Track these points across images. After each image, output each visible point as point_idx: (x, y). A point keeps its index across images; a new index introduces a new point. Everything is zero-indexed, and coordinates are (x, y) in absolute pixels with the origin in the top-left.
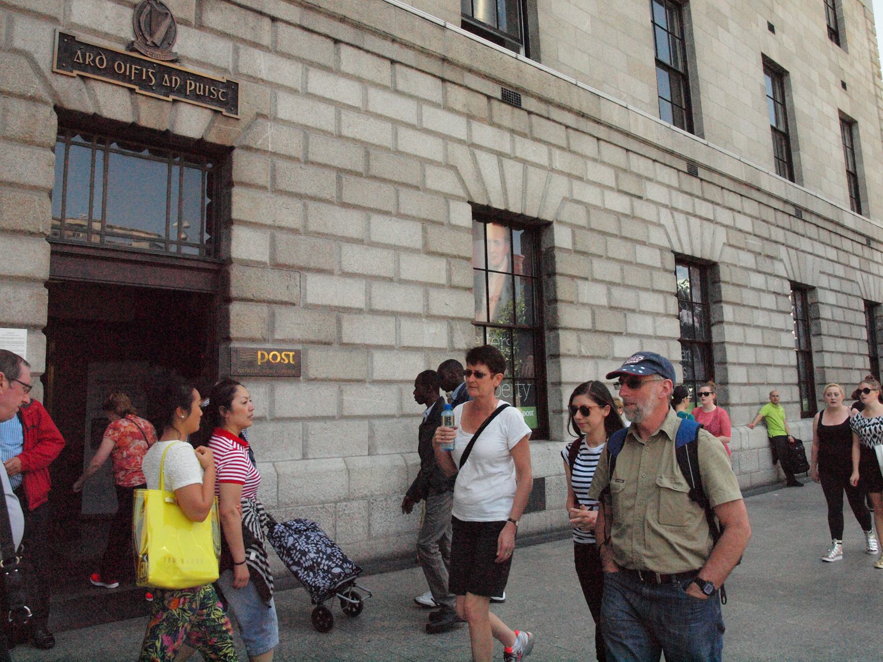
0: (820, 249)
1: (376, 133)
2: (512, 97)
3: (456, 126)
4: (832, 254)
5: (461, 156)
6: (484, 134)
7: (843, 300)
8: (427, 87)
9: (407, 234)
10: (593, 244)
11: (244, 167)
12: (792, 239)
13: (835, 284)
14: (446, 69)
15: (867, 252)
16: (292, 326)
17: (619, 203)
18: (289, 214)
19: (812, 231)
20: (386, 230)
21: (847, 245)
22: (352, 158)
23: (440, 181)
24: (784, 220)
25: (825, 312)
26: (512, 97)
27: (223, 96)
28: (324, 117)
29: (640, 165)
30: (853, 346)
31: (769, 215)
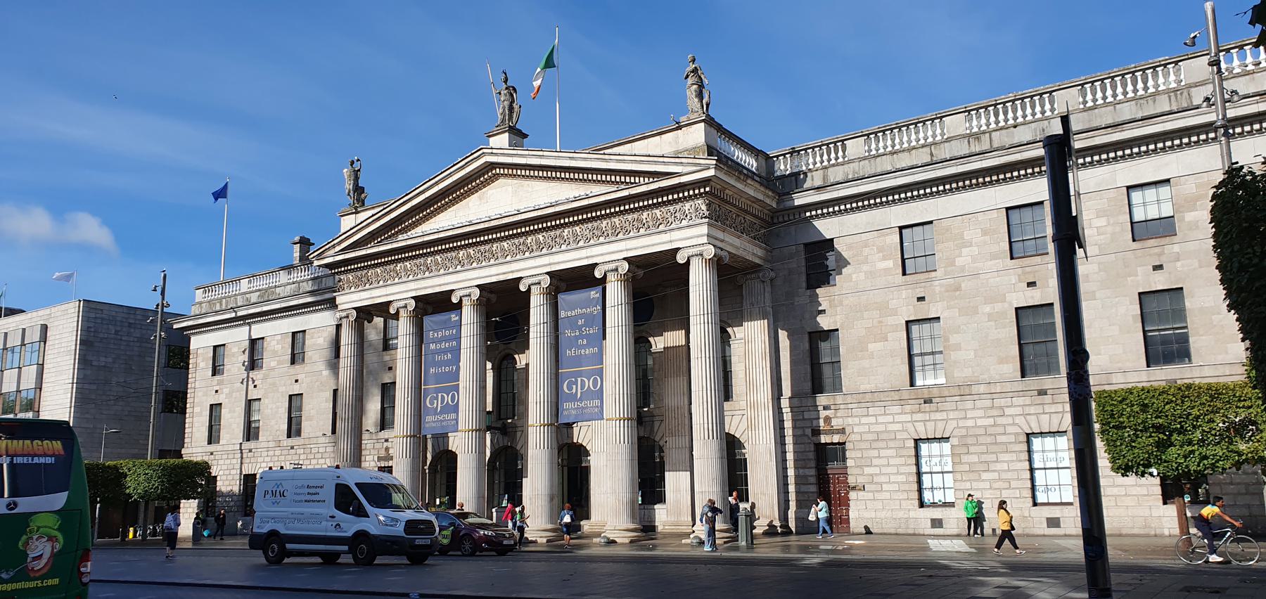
1: (881, 428)
5: (910, 427)
6: (919, 416)
8: (897, 409)
11: (848, 446)
16: (861, 480)
17: (991, 421)
23: (905, 435)
27: (842, 431)
29: (1002, 402)
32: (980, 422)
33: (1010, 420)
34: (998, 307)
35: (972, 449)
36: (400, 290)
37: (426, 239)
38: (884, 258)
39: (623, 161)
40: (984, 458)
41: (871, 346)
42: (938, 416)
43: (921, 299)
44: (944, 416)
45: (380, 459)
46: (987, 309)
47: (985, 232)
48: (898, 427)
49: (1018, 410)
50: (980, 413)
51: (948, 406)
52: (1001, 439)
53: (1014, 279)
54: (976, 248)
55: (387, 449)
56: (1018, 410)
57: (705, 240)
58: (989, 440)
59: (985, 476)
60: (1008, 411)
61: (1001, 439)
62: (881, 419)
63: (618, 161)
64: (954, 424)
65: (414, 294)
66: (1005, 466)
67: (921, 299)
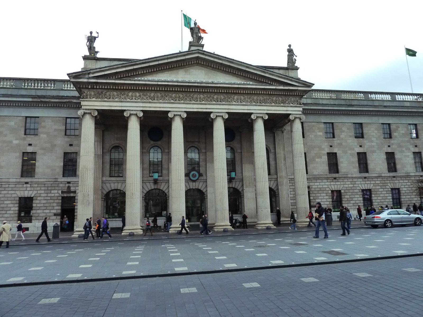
1: (321, 187)
2: (335, 178)
3: (329, 183)
4: (407, 181)
5: (330, 186)
6: (332, 183)
8: (326, 181)
9: (325, 195)
10: (347, 191)
14: (327, 179)
17: (352, 186)
18: (314, 195)
20: (322, 195)
22: (319, 189)
26: (335, 178)
28: (316, 187)
32: (350, 186)
33: (357, 185)
34: (353, 152)
35: (348, 194)
36: (134, 106)
37: (159, 83)
38: (319, 132)
39: (272, 75)
40: (351, 196)
41: (317, 160)
42: (337, 183)
43: (331, 146)
44: (339, 183)
45: (63, 192)
46: (349, 152)
47: (348, 129)
48: (326, 186)
49: (359, 183)
50: (349, 183)
51: (341, 180)
52: (355, 191)
53: (356, 144)
54: (346, 133)
55: (69, 187)
56: (359, 183)
57: (301, 113)
58: (352, 191)
59: (351, 202)
60: (357, 183)
61: (355, 191)
62: (321, 184)
63: (270, 74)
64: (342, 186)
65: (142, 109)
66: (356, 199)
67: (331, 146)
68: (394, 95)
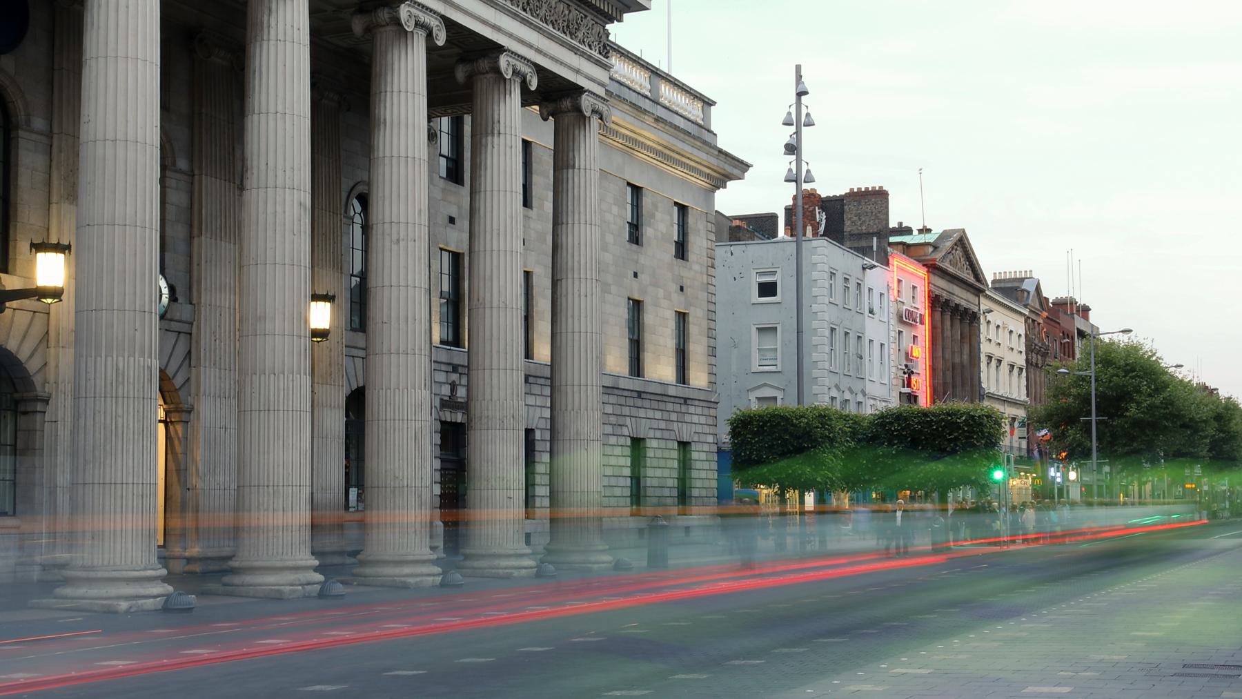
0: (650, 414)
4: (658, 415)
7: (663, 444)
12: (634, 412)
13: (658, 434)
15: (684, 408)
19: (647, 404)
21: (670, 407)
24: (630, 402)
25: (650, 453)
30: (666, 473)
31: (622, 401)
68: (656, 80)
